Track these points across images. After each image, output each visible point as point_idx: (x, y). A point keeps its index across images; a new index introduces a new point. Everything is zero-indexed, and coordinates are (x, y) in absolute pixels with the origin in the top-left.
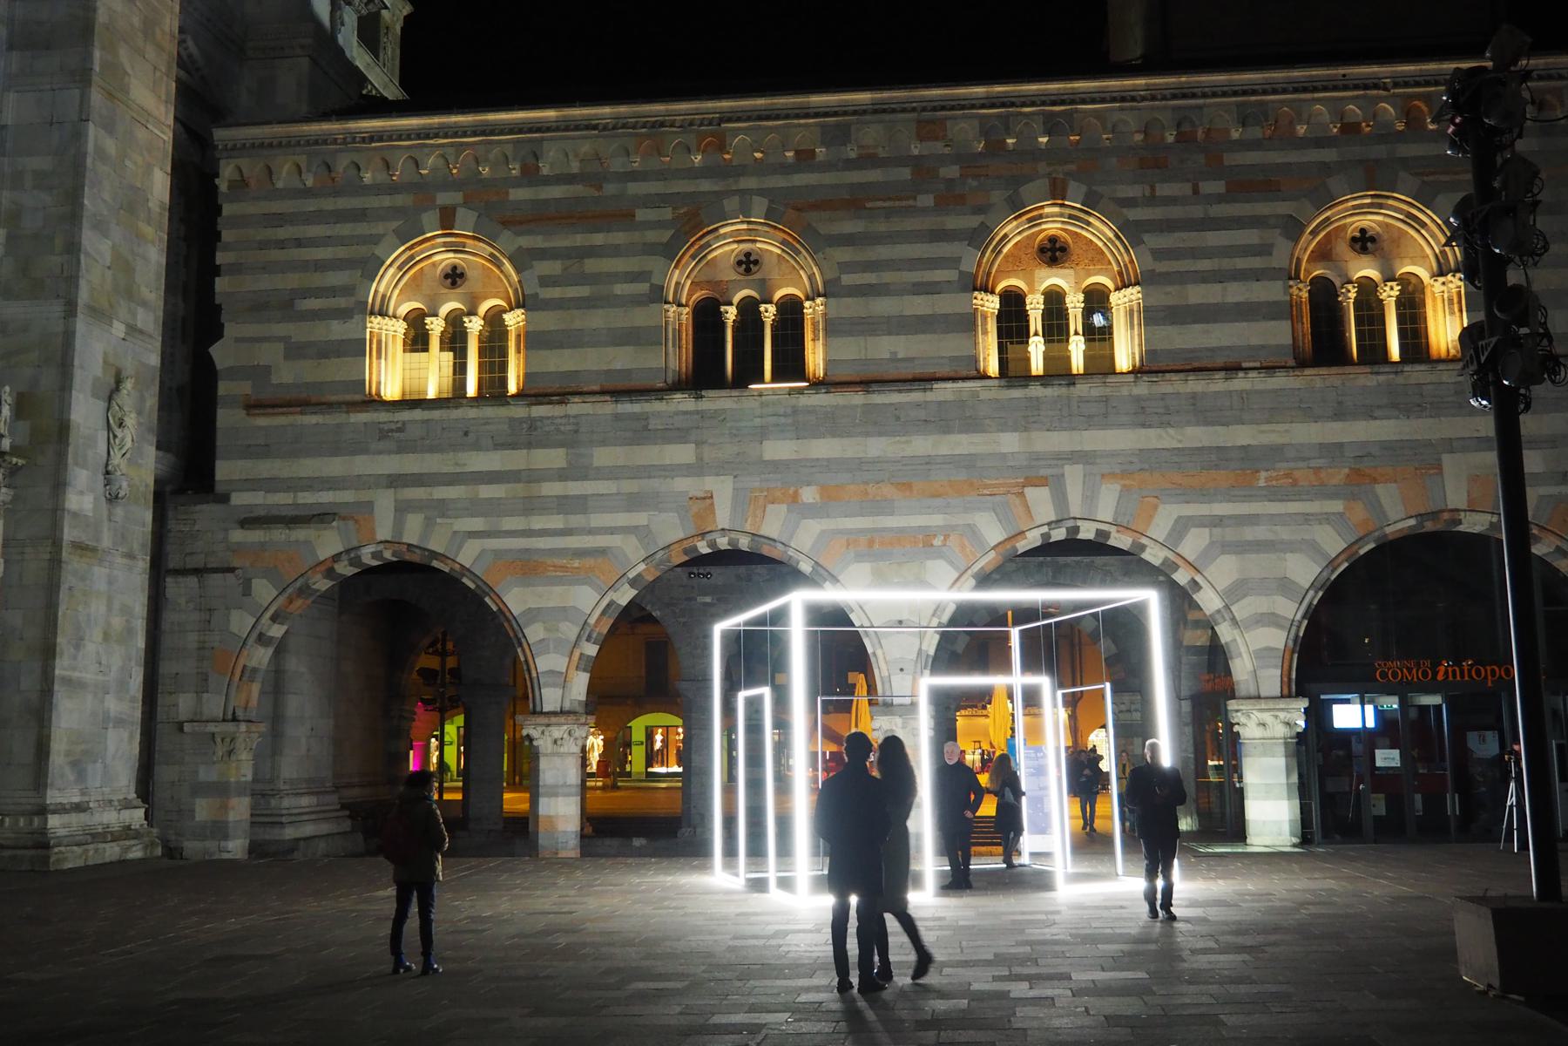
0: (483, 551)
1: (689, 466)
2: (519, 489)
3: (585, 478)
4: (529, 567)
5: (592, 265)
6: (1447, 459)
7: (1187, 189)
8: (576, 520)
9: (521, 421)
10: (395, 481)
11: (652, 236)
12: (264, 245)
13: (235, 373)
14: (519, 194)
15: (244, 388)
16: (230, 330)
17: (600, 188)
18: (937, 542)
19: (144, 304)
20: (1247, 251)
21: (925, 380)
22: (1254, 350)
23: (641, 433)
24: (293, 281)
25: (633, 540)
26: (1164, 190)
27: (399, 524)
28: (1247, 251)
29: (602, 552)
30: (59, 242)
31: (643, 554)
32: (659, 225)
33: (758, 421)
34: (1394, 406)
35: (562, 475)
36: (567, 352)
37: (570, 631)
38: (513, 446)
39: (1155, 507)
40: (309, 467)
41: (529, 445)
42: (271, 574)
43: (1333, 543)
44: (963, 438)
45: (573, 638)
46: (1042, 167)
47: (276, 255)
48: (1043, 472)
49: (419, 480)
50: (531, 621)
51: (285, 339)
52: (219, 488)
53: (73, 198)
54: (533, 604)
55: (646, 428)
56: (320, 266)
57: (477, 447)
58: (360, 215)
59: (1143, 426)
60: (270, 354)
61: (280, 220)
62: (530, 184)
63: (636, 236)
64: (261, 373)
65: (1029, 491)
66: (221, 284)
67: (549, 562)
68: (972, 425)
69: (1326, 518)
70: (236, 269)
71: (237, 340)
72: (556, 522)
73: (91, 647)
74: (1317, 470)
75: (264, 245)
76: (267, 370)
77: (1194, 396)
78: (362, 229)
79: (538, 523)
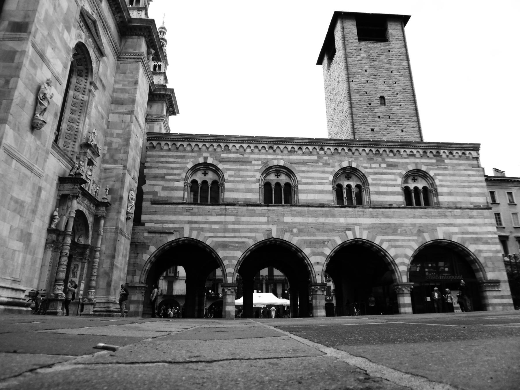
0: (213, 241)
1: (265, 222)
2: (222, 226)
3: (240, 224)
4: (225, 246)
5: (241, 173)
6: (438, 228)
7: (378, 165)
8: (237, 234)
9: (223, 209)
10: (190, 222)
11: (256, 167)
12: (158, 162)
13: (148, 193)
14: (224, 155)
15: (151, 197)
16: (148, 182)
17: (243, 155)
18: (326, 243)
19: (136, 171)
20: (392, 180)
21: (322, 206)
22: (395, 202)
23: (254, 214)
24: (165, 171)
25: (251, 240)
26: (373, 165)
27: (190, 234)
28: (392, 180)
29: (244, 242)
30: (122, 151)
32: (258, 165)
33: (282, 212)
34: (426, 216)
35: (234, 223)
36: (235, 193)
37: (235, 262)
38: (221, 215)
39: (376, 237)
40: (166, 218)
41: (225, 215)
42: (154, 245)
43: (416, 247)
44: (331, 219)
45: (236, 264)
46: (346, 158)
47: (160, 165)
48: (350, 228)
49: (196, 222)
50: (225, 260)
51: (162, 185)
52: (142, 221)
53: (127, 141)
54: (225, 255)
55: (255, 213)
56: (172, 168)
57: (211, 215)
58: (184, 157)
59: (372, 217)
60: (157, 189)
61: (163, 156)
62: (226, 153)
63: (253, 167)
64: (155, 193)
65: (347, 232)
66: (146, 171)
68: (333, 216)
69: (413, 240)
70: (150, 167)
71: (149, 185)
72: (232, 235)
73: (120, 258)
74: (411, 230)
75: (158, 162)
76: (157, 192)
77: (382, 212)
78: (184, 160)
79: (227, 235)
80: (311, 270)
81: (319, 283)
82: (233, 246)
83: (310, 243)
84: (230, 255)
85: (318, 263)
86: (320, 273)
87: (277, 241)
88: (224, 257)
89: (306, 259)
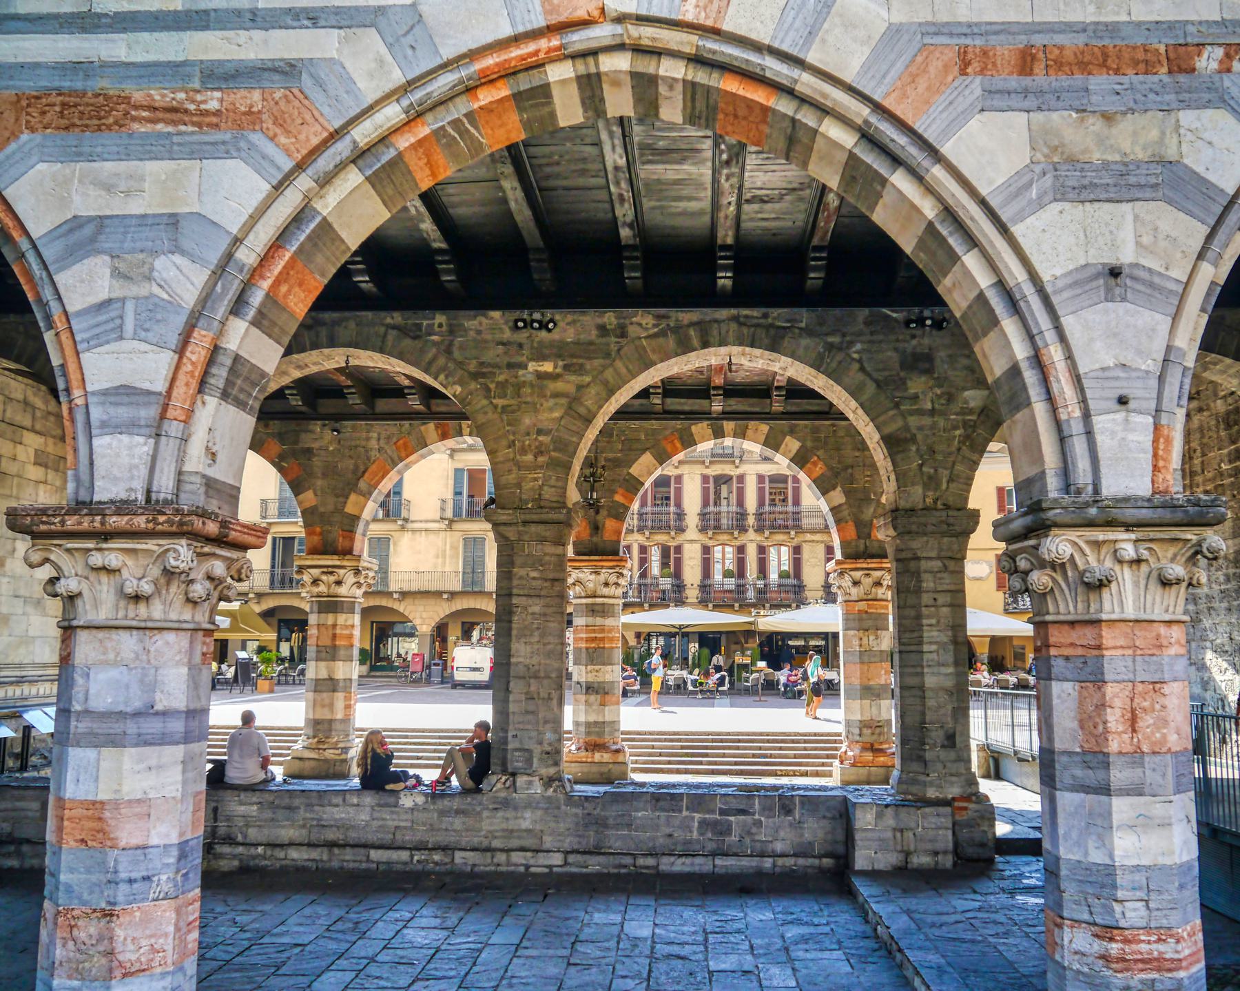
18: (1209, 61)
29: (289, 70)
31: (397, 77)
37: (182, 279)
45: (189, 297)
67: (138, 96)
80: (1037, 360)
81: (1126, 501)
82: (174, 112)
83: (1026, 62)
84: (136, 207)
85: (1115, 272)
86: (1143, 393)
87: (657, 53)
88: (76, 223)
89: (972, 242)
